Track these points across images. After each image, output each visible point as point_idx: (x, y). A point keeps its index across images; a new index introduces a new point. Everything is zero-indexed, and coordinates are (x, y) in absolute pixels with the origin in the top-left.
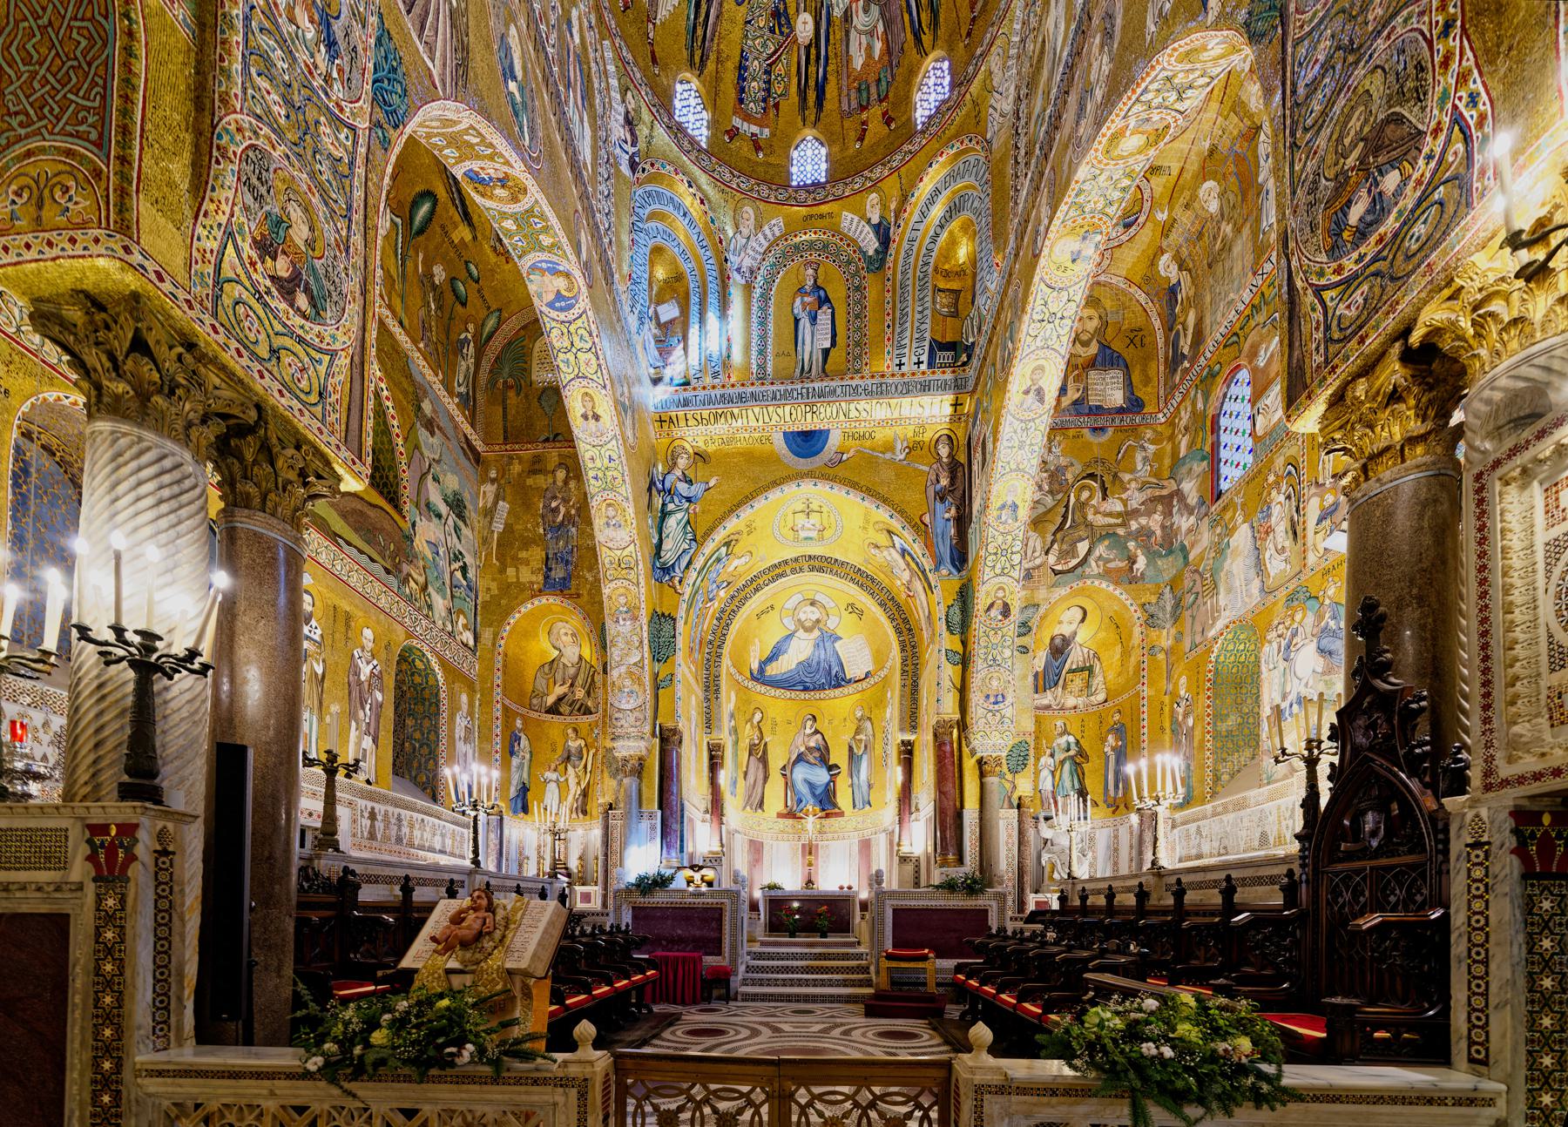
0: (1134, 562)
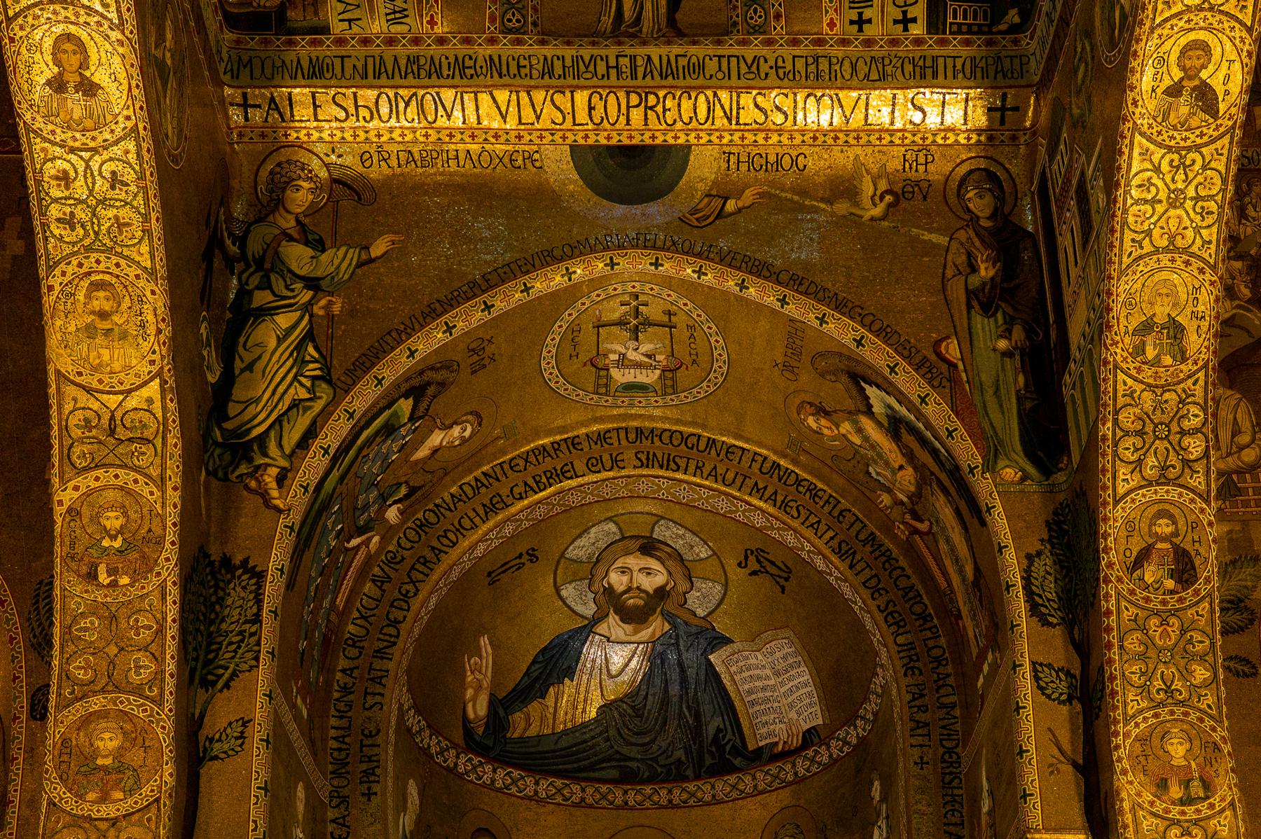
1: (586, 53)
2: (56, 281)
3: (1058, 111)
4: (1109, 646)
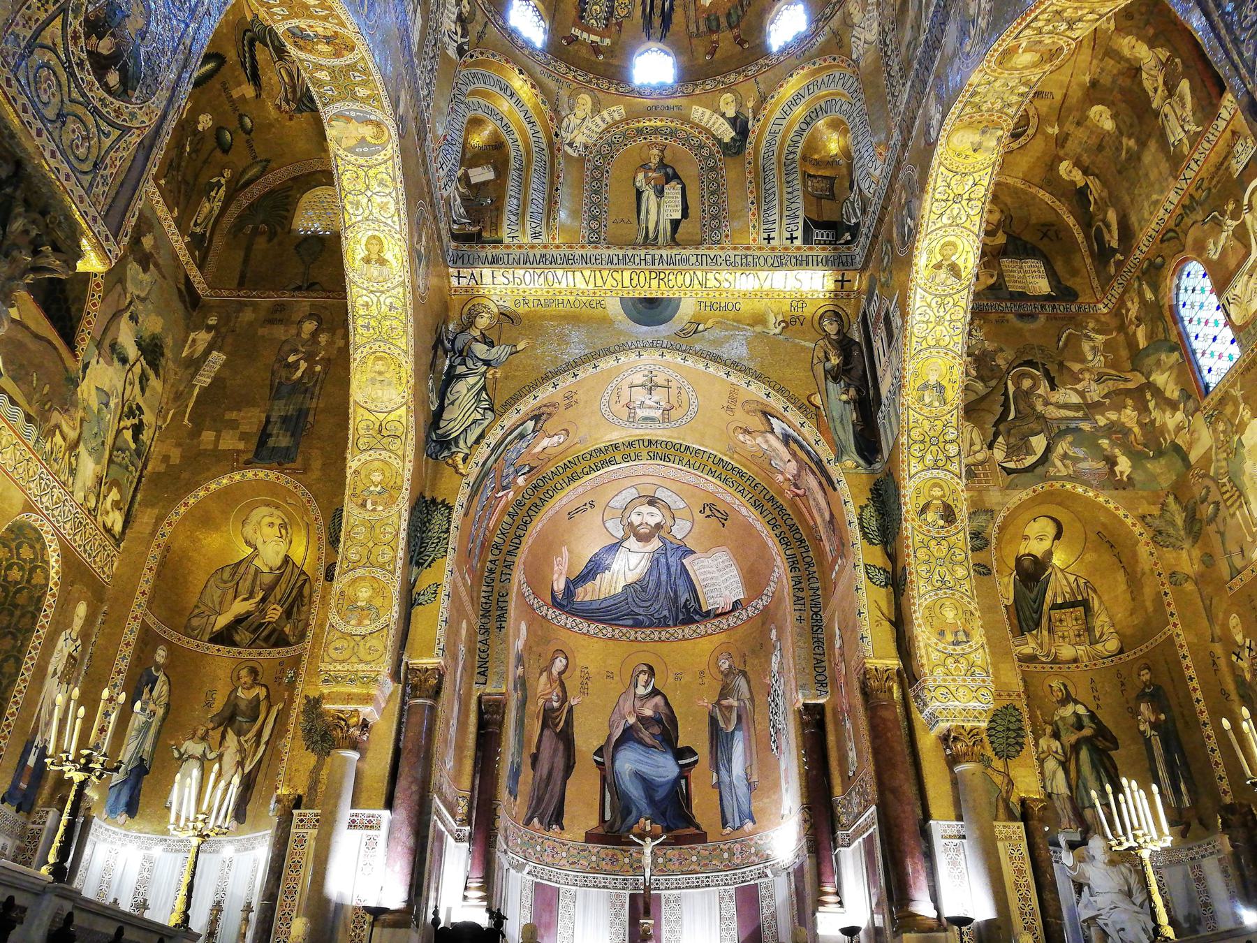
0: (1114, 463)
1: (630, 253)
2: (358, 356)
3: (873, 282)
4: (908, 555)
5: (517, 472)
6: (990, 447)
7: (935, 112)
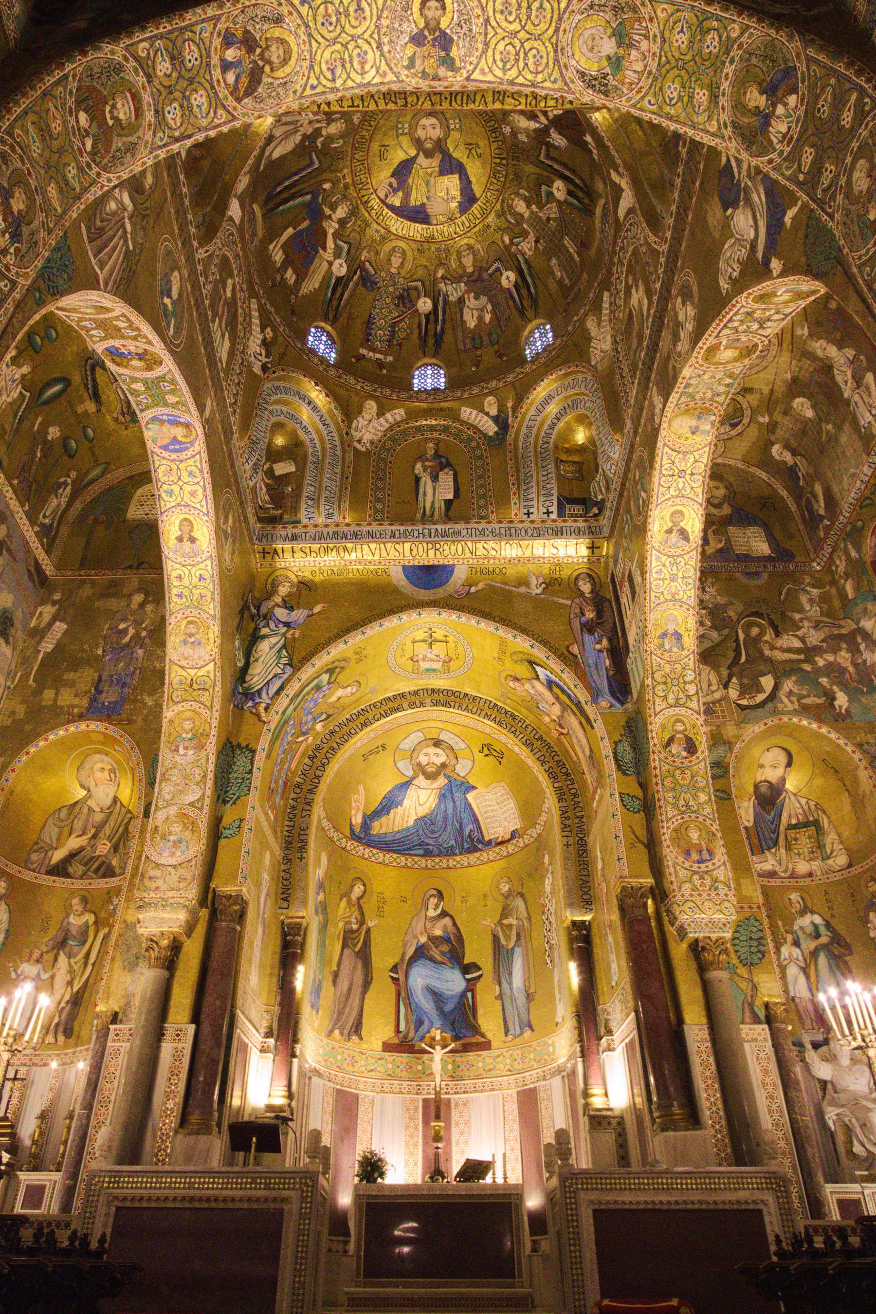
0: (834, 699)
4: (657, 784)
5: (315, 719)
6: (726, 686)
7: (657, 401)
